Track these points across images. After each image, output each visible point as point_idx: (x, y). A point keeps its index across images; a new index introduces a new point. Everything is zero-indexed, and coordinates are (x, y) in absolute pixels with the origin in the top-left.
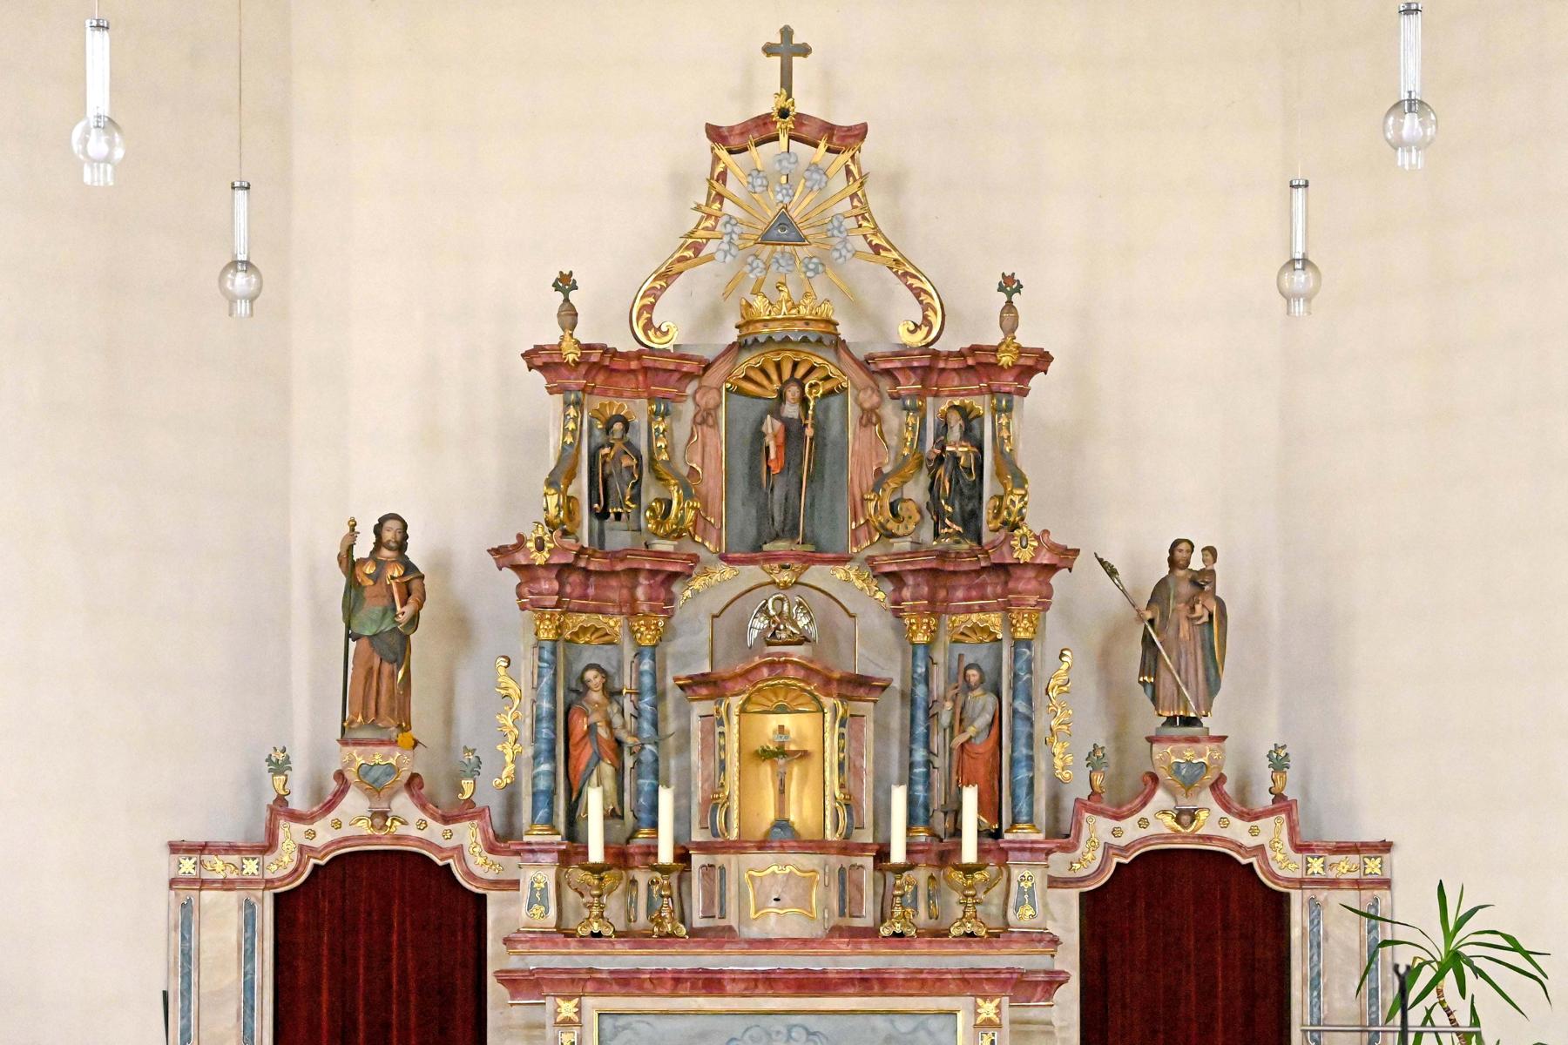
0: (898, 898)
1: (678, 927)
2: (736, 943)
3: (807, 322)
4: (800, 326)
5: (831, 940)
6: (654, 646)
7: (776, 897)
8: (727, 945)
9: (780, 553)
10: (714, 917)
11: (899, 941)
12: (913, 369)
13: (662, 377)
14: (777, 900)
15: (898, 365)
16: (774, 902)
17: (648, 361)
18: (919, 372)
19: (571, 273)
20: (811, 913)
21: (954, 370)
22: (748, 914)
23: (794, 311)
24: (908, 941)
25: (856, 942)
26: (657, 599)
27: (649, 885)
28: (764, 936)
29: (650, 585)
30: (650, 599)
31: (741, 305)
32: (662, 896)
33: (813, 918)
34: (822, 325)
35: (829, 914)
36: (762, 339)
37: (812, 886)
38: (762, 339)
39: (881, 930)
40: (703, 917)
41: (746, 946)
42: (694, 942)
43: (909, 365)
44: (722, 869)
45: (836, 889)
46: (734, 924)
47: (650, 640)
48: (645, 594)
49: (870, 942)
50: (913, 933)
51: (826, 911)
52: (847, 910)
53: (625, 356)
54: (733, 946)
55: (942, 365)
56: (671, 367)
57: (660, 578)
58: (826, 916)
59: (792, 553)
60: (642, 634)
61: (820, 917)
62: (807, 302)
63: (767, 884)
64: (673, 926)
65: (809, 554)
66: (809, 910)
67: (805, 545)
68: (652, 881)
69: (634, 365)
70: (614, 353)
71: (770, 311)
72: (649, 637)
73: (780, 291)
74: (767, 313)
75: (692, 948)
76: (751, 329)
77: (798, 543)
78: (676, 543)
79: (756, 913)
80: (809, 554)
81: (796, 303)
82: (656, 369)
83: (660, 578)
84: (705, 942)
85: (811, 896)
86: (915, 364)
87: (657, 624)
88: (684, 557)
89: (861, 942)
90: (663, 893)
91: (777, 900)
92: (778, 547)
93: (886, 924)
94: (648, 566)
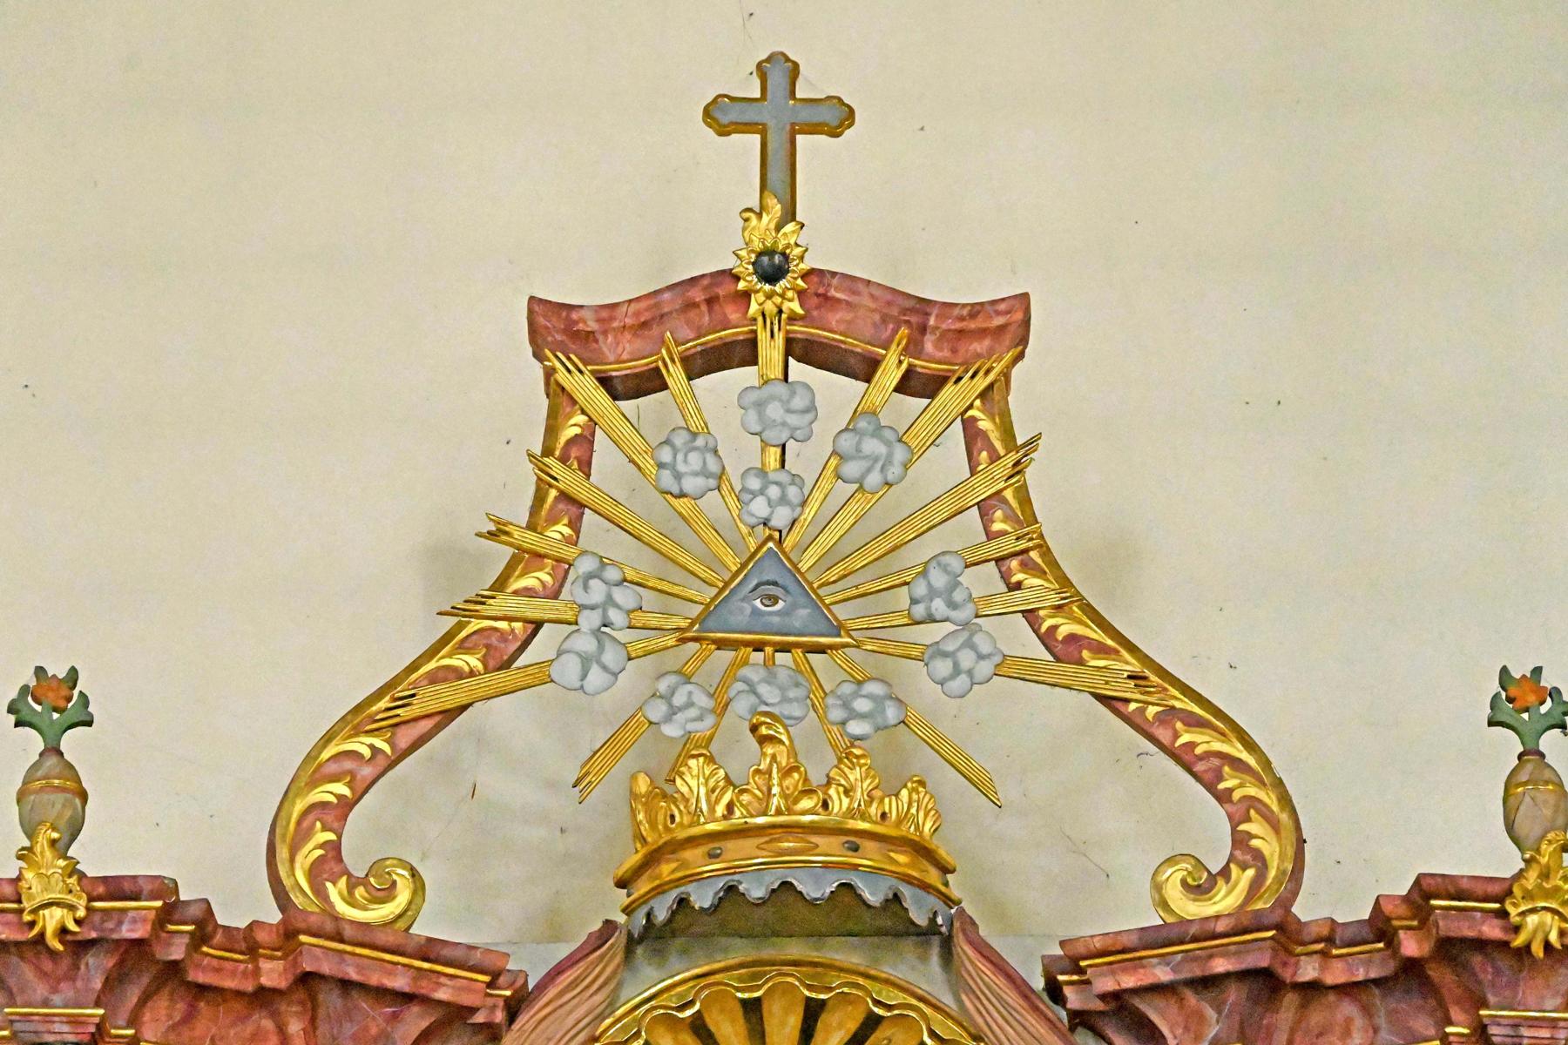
3: (854, 840)
4: (830, 849)
12: (1207, 983)
13: (374, 1016)
15: (1163, 975)
17: (317, 955)
18: (1234, 994)
19: (73, 672)
21: (1347, 990)
23: (806, 803)
31: (634, 796)
34: (902, 858)
36: (702, 898)
38: (702, 898)
43: (1198, 972)
53: (248, 942)
55: (1308, 971)
56: (400, 983)
62: (854, 775)
69: (273, 973)
70: (205, 927)
71: (730, 807)
73: (764, 740)
74: (720, 810)
76: (666, 870)
81: (817, 779)
82: (346, 985)
86: (1220, 966)
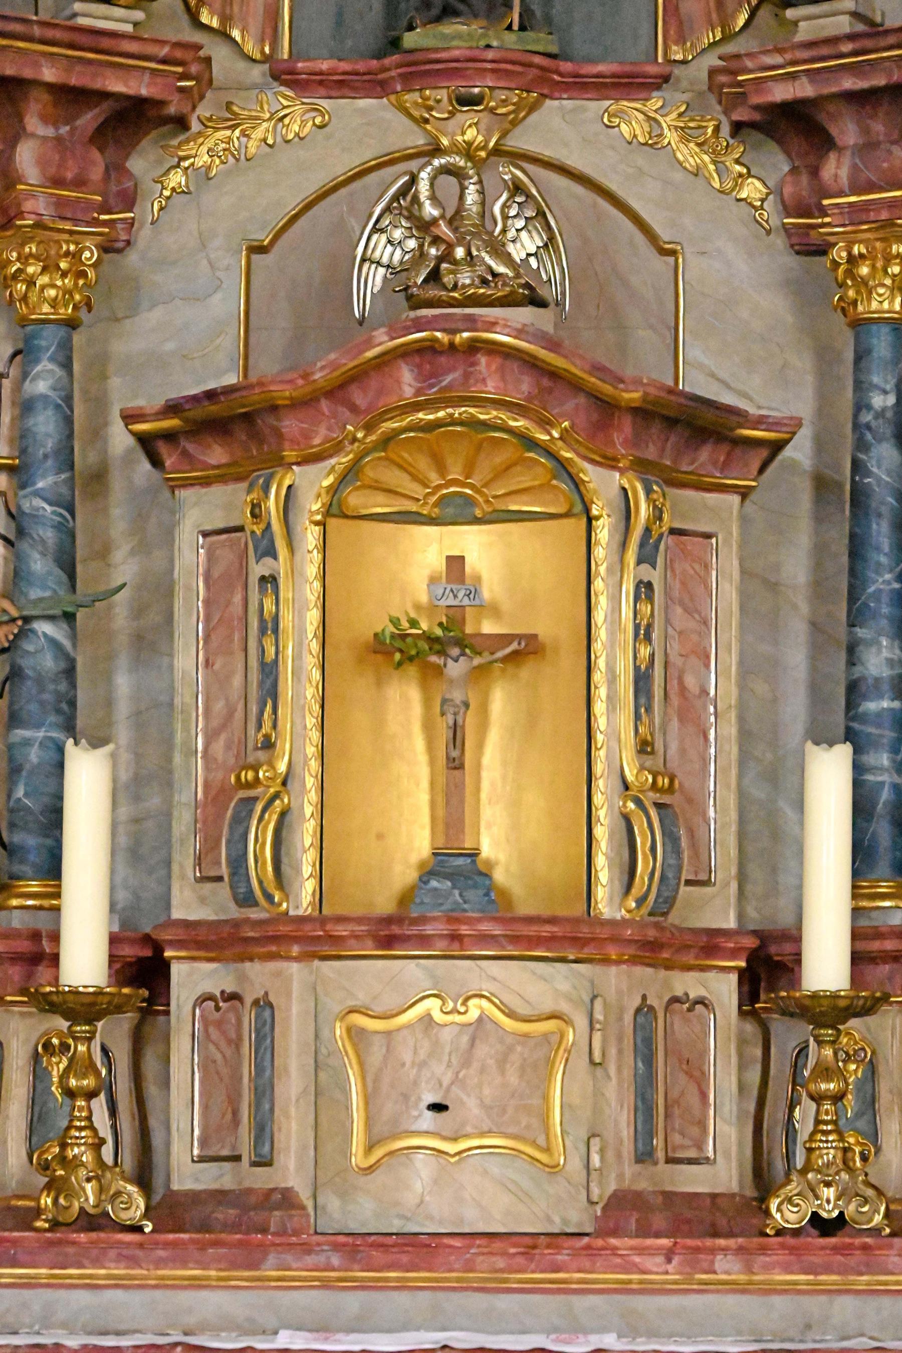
0: (827, 1106)
1: (118, 1193)
2: (307, 1249)
5: (613, 1241)
6: (72, 324)
7: (431, 1098)
8: (272, 1259)
9: (456, 53)
10: (237, 1158)
11: (836, 1249)
14: (438, 1108)
16: (429, 1114)
20: (547, 1150)
22: (345, 1152)
24: (865, 1248)
25: (697, 1250)
26: (79, 183)
27: (36, 1057)
28: (396, 1226)
29: (59, 139)
30: (58, 182)
32: (70, 1094)
33: (553, 1169)
35: (602, 1152)
37: (550, 1063)
39: (773, 1208)
40: (202, 1159)
41: (335, 1260)
42: (167, 1245)
44: (264, 1004)
45: (628, 1073)
46: (305, 1196)
47: (54, 303)
48: (42, 162)
49: (740, 1250)
50: (878, 1218)
51: (595, 1144)
52: (658, 1142)
54: (289, 1258)
57: (89, 120)
58: (596, 1160)
59: (490, 55)
60: (31, 283)
61: (575, 1164)
63: (407, 1057)
64: (101, 1190)
65: (537, 60)
66: (541, 1141)
67: (530, 34)
68: (47, 1046)
72: (52, 293)
75: (159, 1263)
77: (509, 28)
78: (139, 15)
79: (369, 1148)
80: (537, 60)
83: (89, 120)
84: (203, 1247)
85: (546, 1098)
87: (76, 256)
88: (164, 51)
89: (713, 1251)
90: (73, 1082)
91: (438, 1108)
92: (444, 37)
93: (792, 1188)
94: (49, 74)
